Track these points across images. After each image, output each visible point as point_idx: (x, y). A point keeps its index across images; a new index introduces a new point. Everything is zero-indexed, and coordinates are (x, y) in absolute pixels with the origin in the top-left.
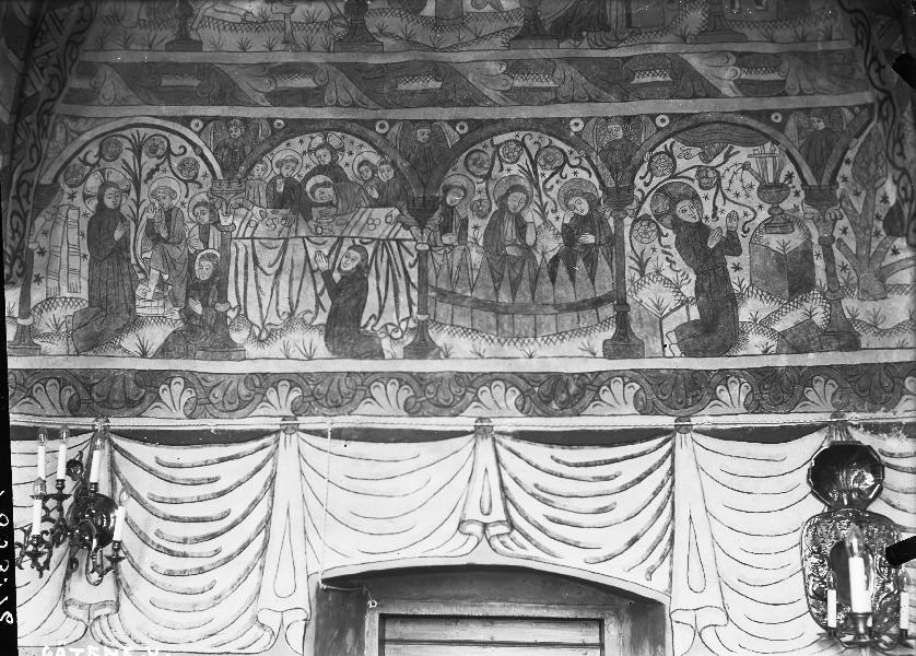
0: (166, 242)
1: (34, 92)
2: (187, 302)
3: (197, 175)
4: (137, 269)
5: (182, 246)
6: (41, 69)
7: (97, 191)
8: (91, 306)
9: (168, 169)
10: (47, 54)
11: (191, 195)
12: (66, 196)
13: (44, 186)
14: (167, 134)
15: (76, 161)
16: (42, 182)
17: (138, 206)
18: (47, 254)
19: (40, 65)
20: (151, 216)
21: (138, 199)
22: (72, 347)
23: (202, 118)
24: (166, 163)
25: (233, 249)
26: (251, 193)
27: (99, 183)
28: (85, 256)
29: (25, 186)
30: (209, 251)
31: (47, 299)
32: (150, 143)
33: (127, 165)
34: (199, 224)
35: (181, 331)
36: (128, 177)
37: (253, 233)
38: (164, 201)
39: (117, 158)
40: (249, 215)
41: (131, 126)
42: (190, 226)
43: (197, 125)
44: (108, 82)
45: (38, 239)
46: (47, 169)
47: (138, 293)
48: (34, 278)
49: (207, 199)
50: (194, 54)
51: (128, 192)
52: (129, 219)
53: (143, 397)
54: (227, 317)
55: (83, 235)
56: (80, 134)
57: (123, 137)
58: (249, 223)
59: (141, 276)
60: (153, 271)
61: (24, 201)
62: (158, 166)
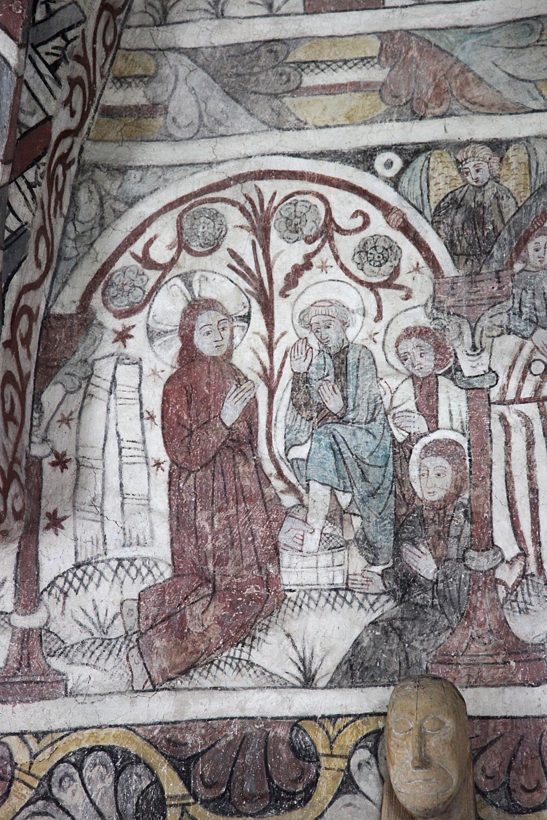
0: (341, 419)
1: (39, 117)
2: (397, 553)
3: (396, 271)
4: (278, 484)
5: (376, 427)
6: (53, 68)
7: (176, 319)
8: (177, 573)
9: (332, 261)
10: (62, 34)
11: (387, 315)
12: (108, 337)
13: (60, 317)
14: (323, 189)
15: (125, 260)
16: (57, 310)
17: (270, 348)
18: (72, 466)
19: (50, 60)
20: (302, 367)
21: (271, 337)
22: (138, 670)
23: (398, 149)
24: (326, 253)
25: (497, 428)
26: (527, 297)
27: (181, 305)
28: (158, 464)
29: (25, 317)
30: (436, 435)
31: (78, 566)
32: (286, 210)
33: (240, 261)
34: (412, 376)
35: (391, 621)
36: (244, 285)
37: (538, 388)
38: (325, 332)
39: (214, 248)
40: (526, 351)
41: (240, 179)
42: (394, 383)
43: (389, 164)
44: (182, 90)
45: (53, 435)
46: (65, 283)
47: (283, 538)
48: (44, 522)
49: (424, 321)
50: (367, 15)
51: (247, 318)
52: (252, 376)
53: (314, 784)
54: (497, 581)
55: (152, 417)
56: (131, 203)
57: (224, 200)
58: (528, 366)
59: (289, 500)
60: (314, 486)
61: (22, 352)
62: (308, 257)
